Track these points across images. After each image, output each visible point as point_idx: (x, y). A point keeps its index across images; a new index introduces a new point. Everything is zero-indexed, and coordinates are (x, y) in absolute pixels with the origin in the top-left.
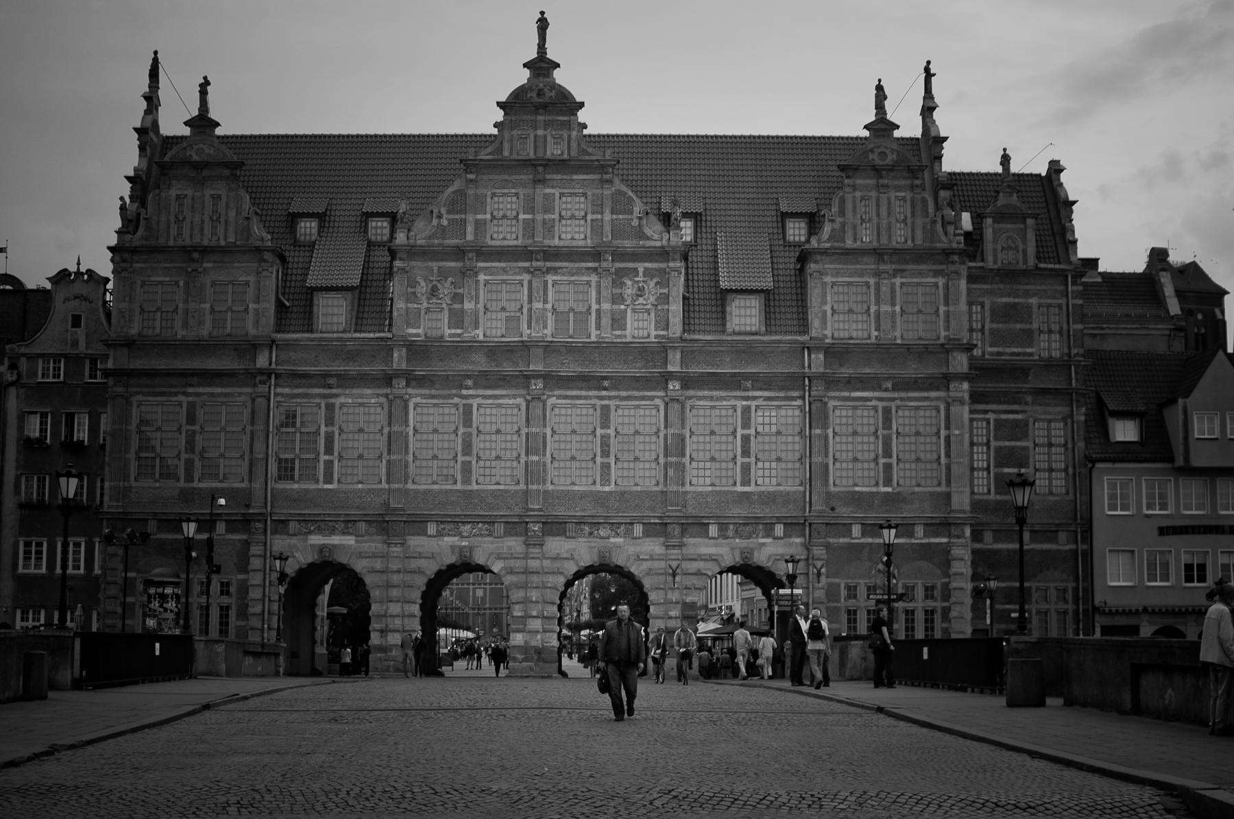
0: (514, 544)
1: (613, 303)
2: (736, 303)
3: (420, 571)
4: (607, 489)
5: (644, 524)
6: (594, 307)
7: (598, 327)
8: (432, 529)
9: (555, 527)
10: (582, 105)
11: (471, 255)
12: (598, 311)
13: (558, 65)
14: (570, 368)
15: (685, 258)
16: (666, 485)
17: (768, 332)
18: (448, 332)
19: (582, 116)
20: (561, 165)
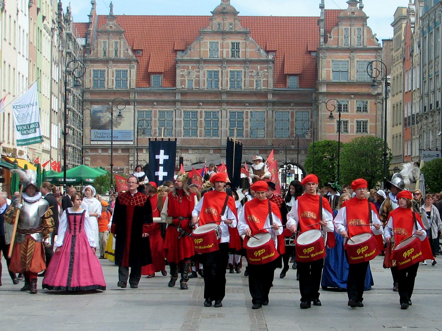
1: (250, 78)
4: (247, 138)
7: (245, 86)
8: (190, 152)
11: (202, 62)
12: (245, 81)
15: (273, 62)
16: (267, 137)
17: (300, 88)
18: (195, 87)
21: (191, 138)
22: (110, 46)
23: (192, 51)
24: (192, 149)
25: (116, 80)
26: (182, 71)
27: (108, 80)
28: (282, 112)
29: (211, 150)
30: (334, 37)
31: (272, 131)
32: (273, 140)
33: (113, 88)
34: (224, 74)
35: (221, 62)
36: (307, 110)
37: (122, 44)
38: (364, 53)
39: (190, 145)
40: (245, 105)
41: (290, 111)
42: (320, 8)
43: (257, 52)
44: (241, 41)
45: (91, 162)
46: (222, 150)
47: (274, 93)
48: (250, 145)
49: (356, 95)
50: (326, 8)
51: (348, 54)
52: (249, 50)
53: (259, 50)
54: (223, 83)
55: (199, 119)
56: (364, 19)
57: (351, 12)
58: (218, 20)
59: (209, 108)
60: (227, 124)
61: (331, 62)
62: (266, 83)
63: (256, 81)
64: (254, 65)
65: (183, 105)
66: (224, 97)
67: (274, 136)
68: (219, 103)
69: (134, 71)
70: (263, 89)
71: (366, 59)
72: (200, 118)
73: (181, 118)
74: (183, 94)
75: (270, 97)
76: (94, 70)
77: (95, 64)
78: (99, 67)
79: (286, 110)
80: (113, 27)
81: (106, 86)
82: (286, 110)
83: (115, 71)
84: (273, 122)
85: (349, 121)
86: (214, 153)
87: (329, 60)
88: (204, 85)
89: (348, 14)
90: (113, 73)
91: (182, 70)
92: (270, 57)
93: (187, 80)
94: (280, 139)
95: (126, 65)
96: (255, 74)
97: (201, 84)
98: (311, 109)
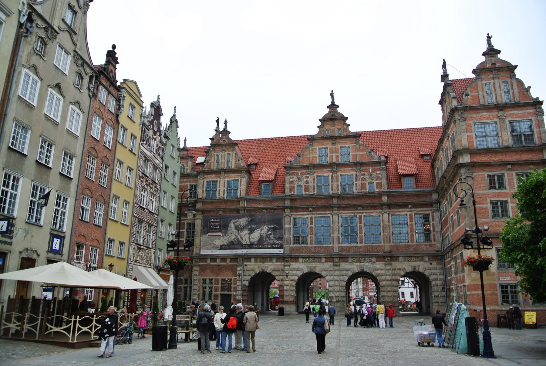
0: (328, 265)
1: (361, 181)
2: (405, 179)
3: (296, 275)
5: (376, 257)
6: (355, 183)
7: (356, 189)
8: (300, 260)
9: (343, 258)
10: (347, 118)
12: (356, 184)
13: (338, 107)
14: (346, 202)
16: (384, 243)
17: (417, 188)
19: (347, 122)
20: (340, 137)
21: (301, 246)
22: (223, 158)
23: (301, 158)
24: (302, 258)
25: (227, 190)
26: (290, 178)
27: (219, 190)
28: (399, 215)
29: (322, 259)
30: (472, 94)
31: (390, 237)
32: (390, 246)
33: (224, 198)
34: (334, 178)
35: (331, 165)
36: (427, 212)
37: (234, 156)
38: (517, 110)
39: (300, 253)
40: (357, 210)
41: (408, 213)
42: (441, 82)
43: (369, 154)
44: (350, 145)
45: (200, 272)
46: (334, 259)
47: (389, 195)
48: (365, 252)
49: (514, 164)
50: (451, 78)
51: (494, 113)
52: (361, 153)
53: (370, 153)
54: (334, 187)
55: (310, 226)
56: (511, 69)
57: (491, 63)
58: (328, 126)
59: (319, 214)
60: (339, 230)
61: (472, 124)
62: (379, 185)
63: (369, 183)
64: (366, 168)
65: (293, 212)
66: (335, 201)
67: (392, 242)
68: (330, 207)
69: (244, 181)
70: (377, 191)
71: (521, 117)
72: (310, 224)
73: (290, 225)
74: (293, 199)
75: (385, 199)
76: (207, 182)
77: (208, 176)
78: (211, 178)
79: (404, 213)
80: (226, 141)
81: (218, 196)
82: (404, 213)
83: (226, 181)
84: (389, 226)
85: (509, 201)
86: (326, 261)
87: (469, 122)
88: (314, 191)
89: (488, 66)
90: (224, 183)
91: (292, 176)
92: (383, 158)
93: (296, 187)
94: (398, 244)
95: (237, 175)
96: (367, 177)
97: (311, 189)
98: (431, 210)
